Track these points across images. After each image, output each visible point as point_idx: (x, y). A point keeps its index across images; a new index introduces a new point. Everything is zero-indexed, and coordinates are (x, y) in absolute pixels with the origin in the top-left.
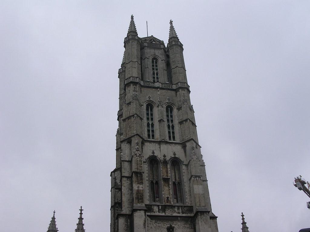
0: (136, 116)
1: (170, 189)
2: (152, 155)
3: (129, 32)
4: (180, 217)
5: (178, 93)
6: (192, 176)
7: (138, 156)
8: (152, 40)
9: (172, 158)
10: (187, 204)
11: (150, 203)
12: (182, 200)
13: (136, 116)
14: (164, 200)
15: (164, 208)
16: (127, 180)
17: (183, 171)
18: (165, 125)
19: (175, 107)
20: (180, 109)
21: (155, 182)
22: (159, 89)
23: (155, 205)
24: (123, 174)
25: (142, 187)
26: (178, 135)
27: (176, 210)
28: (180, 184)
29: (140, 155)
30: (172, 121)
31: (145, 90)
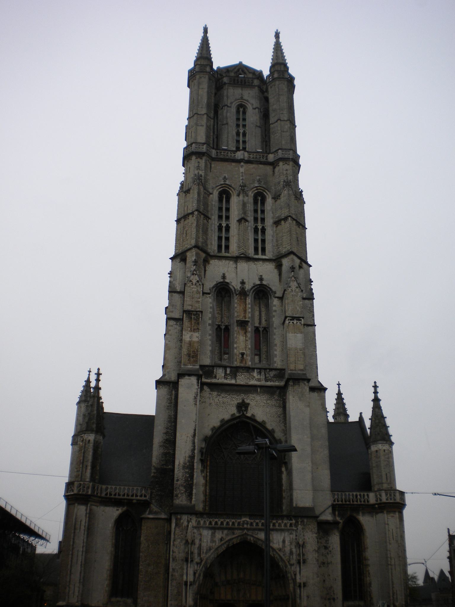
0: (196, 213)
1: (247, 339)
2: (222, 280)
3: (198, 59)
4: (261, 387)
5: (277, 169)
6: (286, 317)
7: (194, 283)
8: (240, 70)
10: (276, 365)
12: (269, 357)
13: (196, 213)
15: (235, 371)
16: (176, 324)
17: (274, 308)
18: (249, 228)
19: (270, 195)
20: (278, 198)
21: (223, 327)
26: (271, 245)
28: (267, 331)
29: (198, 281)
30: (263, 220)
31: (217, 166)
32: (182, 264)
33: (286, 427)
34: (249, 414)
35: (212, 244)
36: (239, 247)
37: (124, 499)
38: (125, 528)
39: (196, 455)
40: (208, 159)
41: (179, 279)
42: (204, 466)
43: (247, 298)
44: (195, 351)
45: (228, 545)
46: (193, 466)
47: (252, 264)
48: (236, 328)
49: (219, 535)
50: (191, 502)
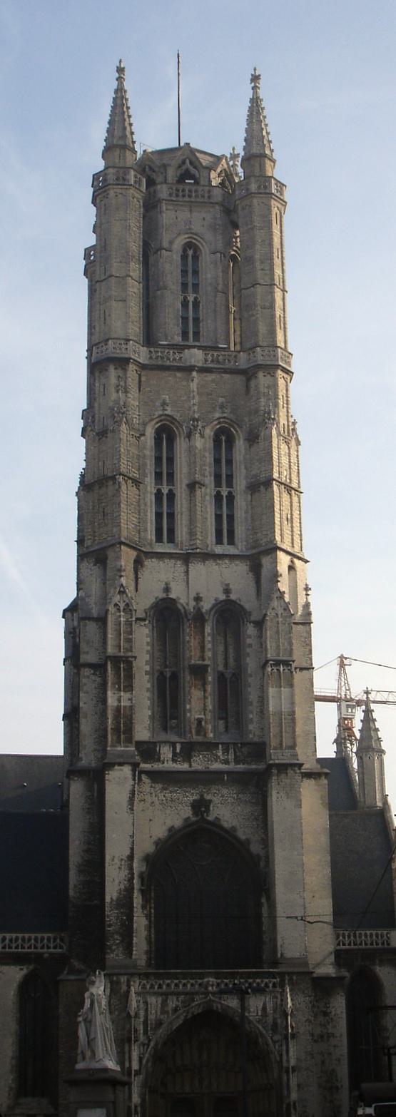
4: (229, 773)
5: (253, 384)
7: (122, 609)
8: (188, 161)
9: (218, 603)
11: (153, 737)
14: (191, 728)
15: (188, 751)
17: (249, 641)
20: (254, 441)
21: (168, 675)
22: (194, 374)
23: (165, 742)
24: (85, 658)
25: (129, 699)
26: (243, 528)
27: (220, 753)
30: (230, 478)
32: (96, 570)
33: (267, 835)
34: (210, 818)
35: (146, 530)
36: (192, 534)
37: (31, 953)
38: (33, 995)
39: (135, 886)
40: (135, 367)
41: (96, 594)
42: (146, 900)
43: (206, 627)
44: (128, 722)
45: (186, 1016)
46: (132, 903)
47: (211, 564)
48: (188, 678)
49: (172, 1002)
50: (131, 958)
